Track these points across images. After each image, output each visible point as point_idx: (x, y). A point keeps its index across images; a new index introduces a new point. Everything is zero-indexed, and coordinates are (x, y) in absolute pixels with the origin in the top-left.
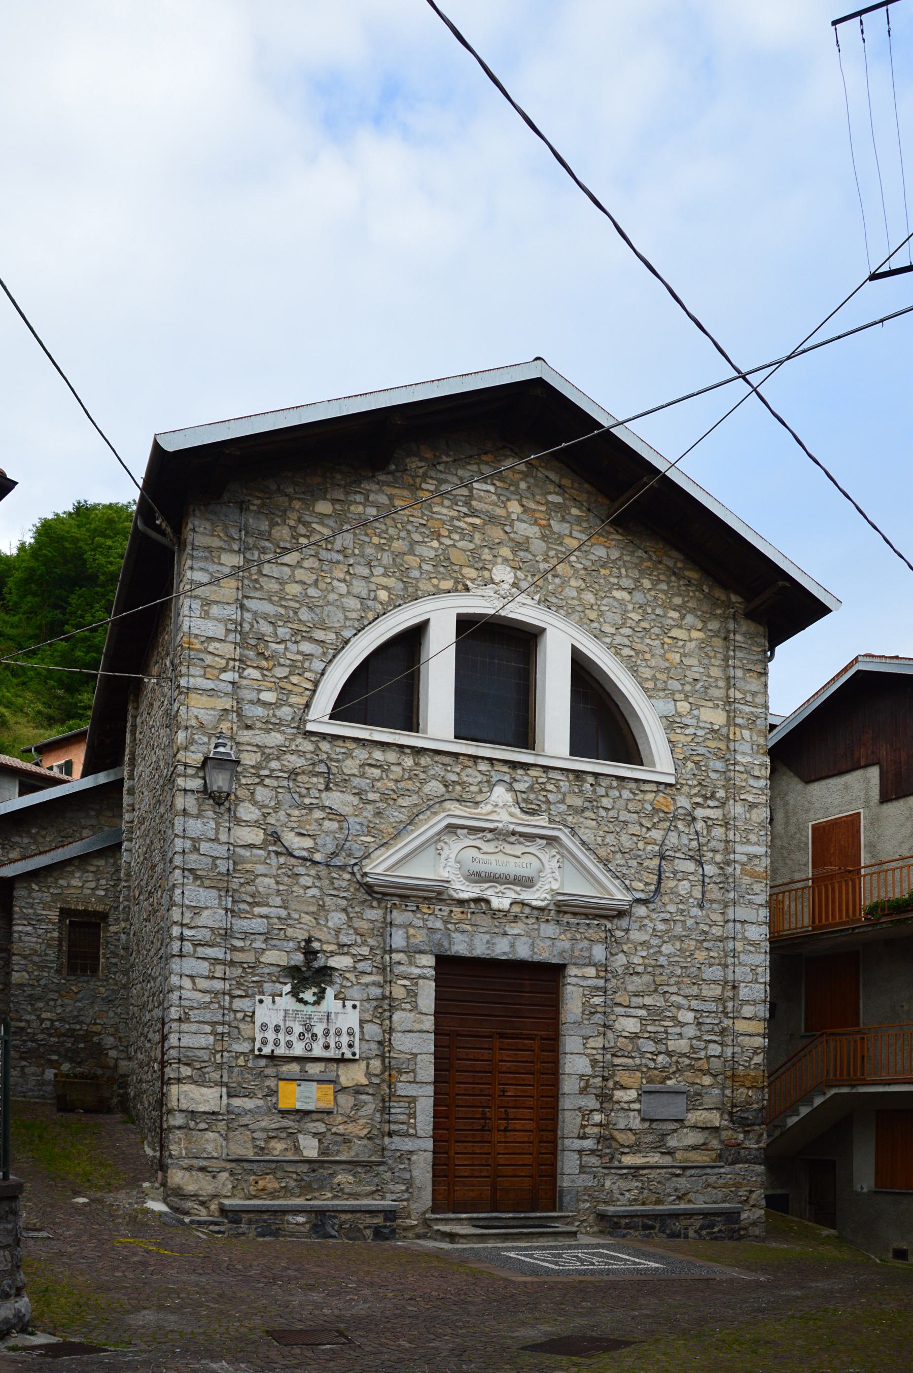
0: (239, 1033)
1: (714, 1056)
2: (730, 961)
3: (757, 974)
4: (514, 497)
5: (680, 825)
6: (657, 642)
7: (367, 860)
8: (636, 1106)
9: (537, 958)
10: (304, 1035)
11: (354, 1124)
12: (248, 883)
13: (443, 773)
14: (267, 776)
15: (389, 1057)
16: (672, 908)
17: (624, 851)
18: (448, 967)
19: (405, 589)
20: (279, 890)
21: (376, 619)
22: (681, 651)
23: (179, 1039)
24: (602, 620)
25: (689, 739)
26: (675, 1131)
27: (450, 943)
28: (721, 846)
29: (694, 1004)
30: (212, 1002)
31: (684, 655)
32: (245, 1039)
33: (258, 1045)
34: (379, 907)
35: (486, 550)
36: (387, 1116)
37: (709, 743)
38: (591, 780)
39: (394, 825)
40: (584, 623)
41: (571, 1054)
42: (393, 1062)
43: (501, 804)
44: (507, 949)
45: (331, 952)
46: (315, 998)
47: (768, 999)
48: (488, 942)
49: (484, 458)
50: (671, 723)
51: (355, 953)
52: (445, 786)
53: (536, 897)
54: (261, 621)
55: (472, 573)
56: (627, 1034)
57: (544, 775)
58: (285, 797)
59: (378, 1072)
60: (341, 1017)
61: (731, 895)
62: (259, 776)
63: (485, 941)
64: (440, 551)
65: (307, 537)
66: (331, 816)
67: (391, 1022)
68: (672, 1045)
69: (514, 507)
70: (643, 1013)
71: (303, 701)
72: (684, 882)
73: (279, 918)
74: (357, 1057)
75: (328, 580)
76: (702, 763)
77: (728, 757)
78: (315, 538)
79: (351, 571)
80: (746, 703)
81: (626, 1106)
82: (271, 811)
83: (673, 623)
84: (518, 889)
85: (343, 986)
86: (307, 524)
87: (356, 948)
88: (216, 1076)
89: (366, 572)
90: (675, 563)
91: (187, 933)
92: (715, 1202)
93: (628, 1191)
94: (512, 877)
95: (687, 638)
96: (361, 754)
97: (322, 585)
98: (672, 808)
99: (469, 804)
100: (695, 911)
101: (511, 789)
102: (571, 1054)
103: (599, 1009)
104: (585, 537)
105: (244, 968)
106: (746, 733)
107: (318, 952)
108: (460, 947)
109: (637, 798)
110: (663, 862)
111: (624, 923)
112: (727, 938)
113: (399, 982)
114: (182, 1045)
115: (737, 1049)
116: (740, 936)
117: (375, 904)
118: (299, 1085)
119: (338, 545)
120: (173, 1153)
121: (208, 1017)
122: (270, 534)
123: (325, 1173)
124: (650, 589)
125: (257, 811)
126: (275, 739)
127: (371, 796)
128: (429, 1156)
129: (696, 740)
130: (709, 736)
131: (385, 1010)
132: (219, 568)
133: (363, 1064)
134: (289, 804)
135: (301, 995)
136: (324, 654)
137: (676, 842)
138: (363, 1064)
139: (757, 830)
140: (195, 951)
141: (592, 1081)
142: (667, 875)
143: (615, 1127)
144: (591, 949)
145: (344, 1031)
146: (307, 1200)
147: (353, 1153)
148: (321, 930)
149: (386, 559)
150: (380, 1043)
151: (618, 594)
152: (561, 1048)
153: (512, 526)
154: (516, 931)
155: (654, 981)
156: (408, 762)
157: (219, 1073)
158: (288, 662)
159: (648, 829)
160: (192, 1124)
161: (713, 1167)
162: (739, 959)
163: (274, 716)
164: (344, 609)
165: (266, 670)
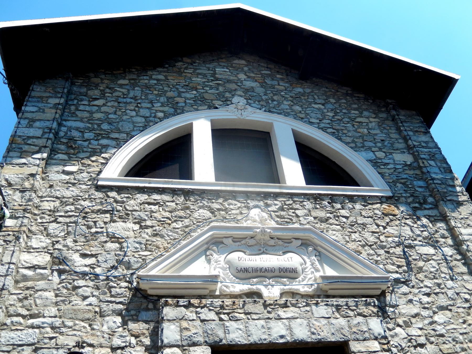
6: (348, 125)
17: (369, 244)
22: (367, 127)
24: (308, 117)
25: (392, 171)
31: (371, 129)
44: (283, 332)
48: (263, 326)
50: (375, 163)
63: (259, 326)
65: (112, 94)
75: (124, 110)
89: (149, 105)
90: (347, 91)
95: (368, 122)
122: (87, 93)
124: (335, 103)
154: (289, 315)
164: (133, 123)
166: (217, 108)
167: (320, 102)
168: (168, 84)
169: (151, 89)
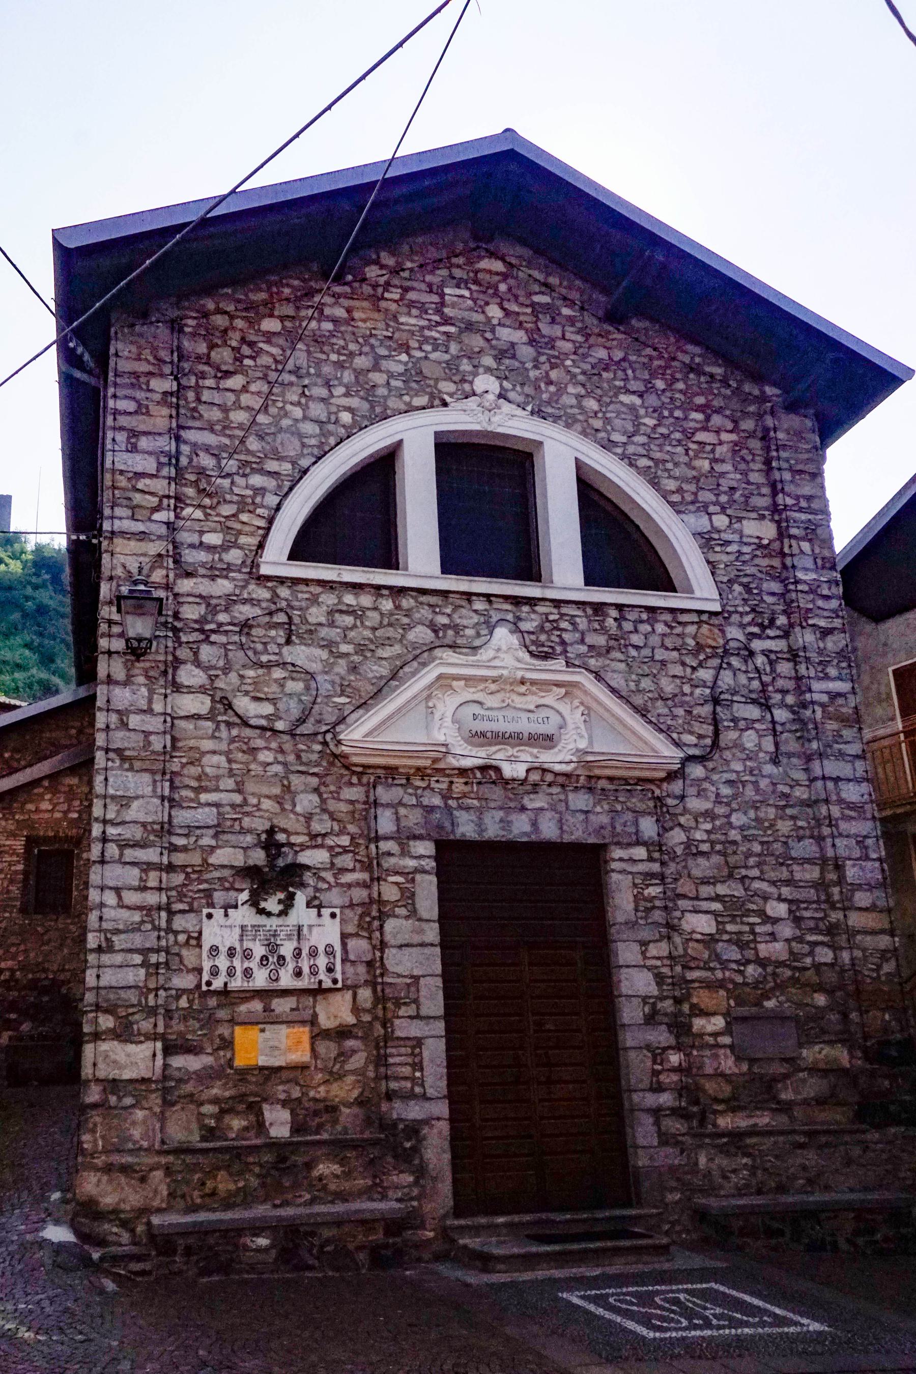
0: (181, 962)
1: (825, 964)
2: (826, 831)
3: (866, 848)
4: (490, 300)
5: (735, 662)
6: (679, 449)
7: (342, 727)
8: (726, 1040)
9: (567, 838)
10: (267, 959)
11: (339, 1083)
12: (192, 763)
13: (430, 617)
14: (213, 631)
15: (382, 983)
16: (738, 767)
18: (454, 856)
19: (372, 408)
20: (231, 770)
21: (338, 444)
23: (98, 976)
24: (609, 428)
25: (732, 557)
26: (786, 1076)
27: (453, 824)
28: (790, 685)
29: (785, 891)
30: (143, 922)
31: (716, 460)
32: (188, 971)
33: (206, 977)
34: (360, 783)
35: (465, 361)
36: (382, 1070)
37: (757, 561)
38: (614, 613)
39: (374, 681)
40: (588, 432)
41: (628, 967)
42: (387, 991)
43: (504, 648)
44: (527, 828)
45: (301, 845)
46: (281, 907)
47: (888, 881)
48: (501, 821)
49: (454, 260)
50: (707, 541)
51: (332, 844)
52: (436, 632)
53: (558, 759)
54: (201, 454)
55: (451, 387)
56: (699, 937)
57: (555, 611)
58: (238, 656)
59: (368, 1005)
60: (318, 929)
61: (815, 745)
62: (202, 631)
63: (497, 819)
64: (410, 365)
66: (295, 675)
67: (382, 934)
68: (764, 950)
69: (494, 311)
70: (717, 906)
71: (253, 541)
72: (750, 732)
73: (233, 806)
74: (339, 985)
75: (280, 405)
76: (752, 586)
77: (784, 574)
78: (265, 360)
79: (307, 393)
80: (801, 510)
81: (711, 1040)
82: (220, 673)
83: (698, 426)
84: (535, 751)
85: (317, 890)
86: (251, 344)
87: (335, 839)
88: (146, 1025)
89: (323, 392)
91: (112, 831)
92: (866, 1189)
93: (734, 1171)
94: (526, 735)
96: (329, 599)
97: (273, 410)
98: (721, 642)
99: (464, 650)
100: (769, 769)
101: (516, 630)
102: (628, 967)
103: (658, 903)
104: (579, 338)
105: (187, 874)
106: (806, 546)
107: (283, 845)
108: (466, 827)
109: (676, 631)
110: (719, 709)
111: (676, 787)
112: (816, 802)
113: (391, 879)
114: (102, 983)
115: (858, 954)
116: (834, 798)
117: (355, 780)
118: (263, 1031)
119: (290, 365)
120: (85, 1146)
121: (137, 940)
122: (208, 355)
123: (300, 1159)
124: (664, 391)
125: (201, 673)
126: (223, 586)
127: (345, 648)
128: (444, 1127)
129: (743, 558)
130: (758, 553)
131: (374, 918)
132: (149, 395)
133: (349, 995)
134: (241, 663)
135: (263, 905)
136: (279, 487)
137: (731, 682)
138: (349, 995)
139: (836, 661)
140: (121, 855)
141: (660, 1005)
142: (726, 724)
143: (700, 1072)
144: (636, 824)
145: (321, 949)
146: (275, 1206)
147: (339, 1128)
148: (287, 817)
149: (348, 376)
150: (370, 964)
151: (625, 398)
152: (613, 959)
153: (493, 331)
154: (538, 805)
155: (727, 862)
156: (387, 605)
157: (152, 1020)
158: (235, 498)
159: (694, 669)
160: (113, 1100)
161: (851, 1132)
162: (837, 828)
163: (221, 560)
164: (301, 436)
165: (210, 508)
166: (445, 404)
167: (635, 389)
168: (354, 334)
169: (326, 348)
